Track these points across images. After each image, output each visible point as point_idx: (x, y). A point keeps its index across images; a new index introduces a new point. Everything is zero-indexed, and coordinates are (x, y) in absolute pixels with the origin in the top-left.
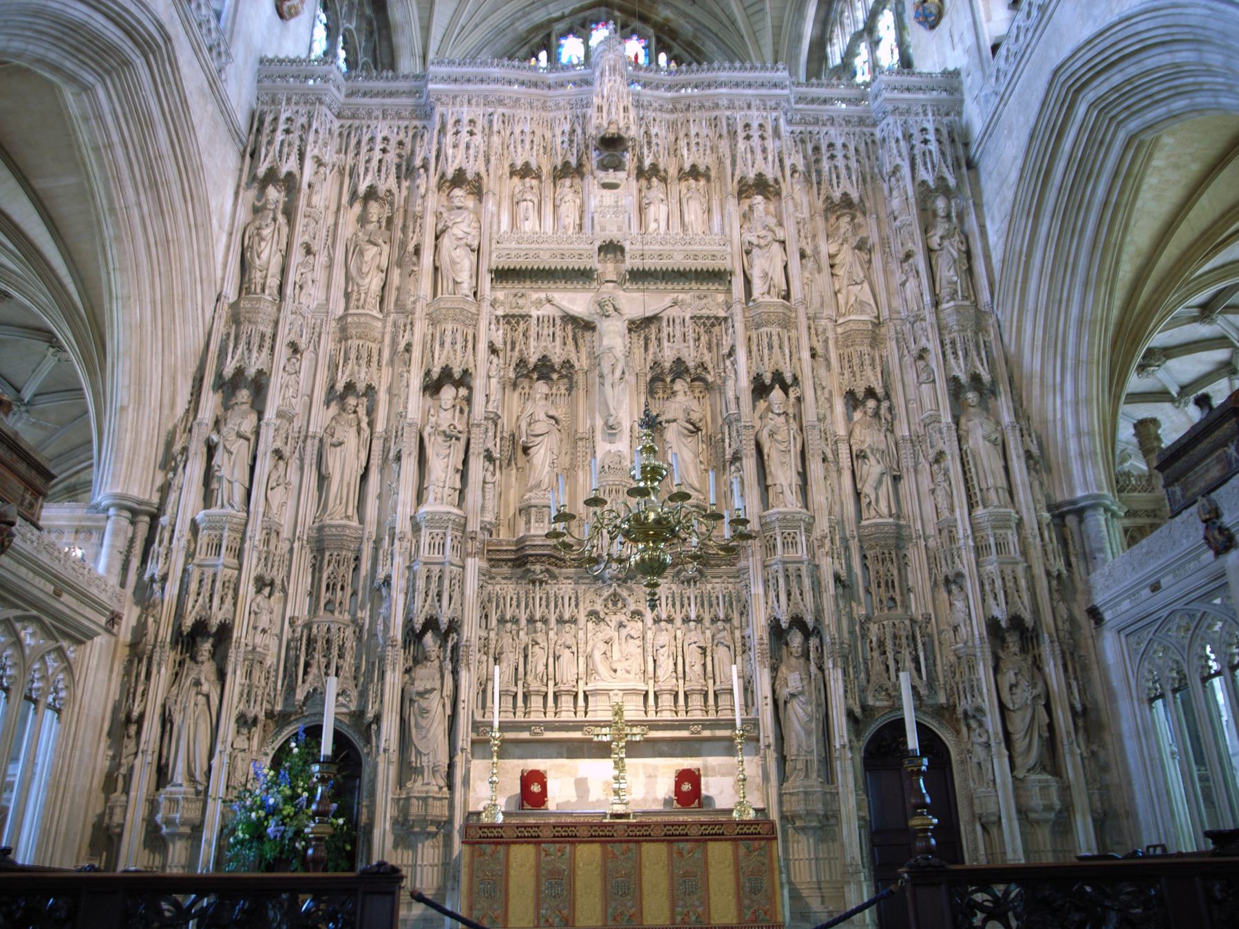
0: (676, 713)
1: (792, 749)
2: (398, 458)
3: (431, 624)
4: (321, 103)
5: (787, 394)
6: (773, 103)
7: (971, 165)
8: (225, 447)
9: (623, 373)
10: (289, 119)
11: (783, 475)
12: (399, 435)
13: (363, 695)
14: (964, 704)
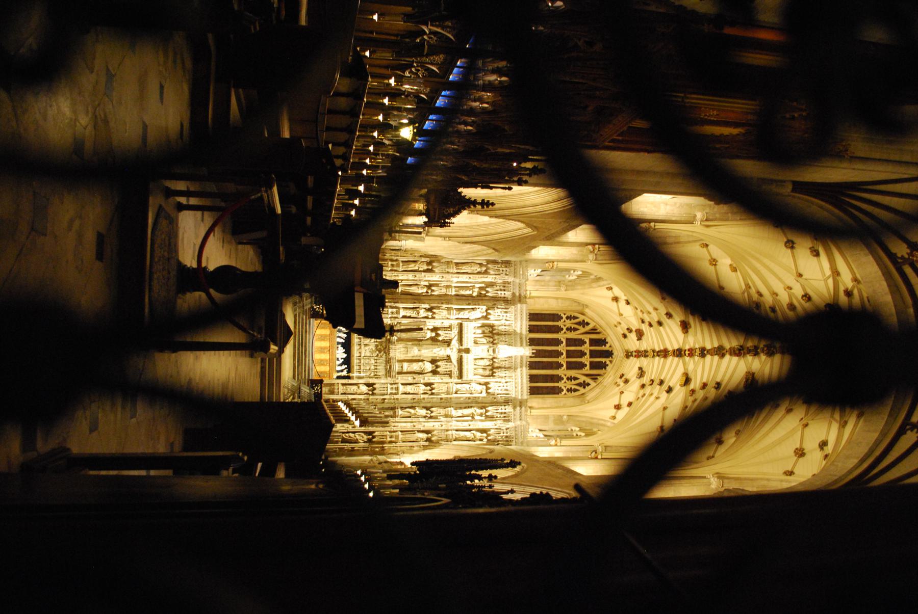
1: (348, 386)
2: (415, 303)
4: (515, 277)
11: (409, 389)
12: (419, 303)
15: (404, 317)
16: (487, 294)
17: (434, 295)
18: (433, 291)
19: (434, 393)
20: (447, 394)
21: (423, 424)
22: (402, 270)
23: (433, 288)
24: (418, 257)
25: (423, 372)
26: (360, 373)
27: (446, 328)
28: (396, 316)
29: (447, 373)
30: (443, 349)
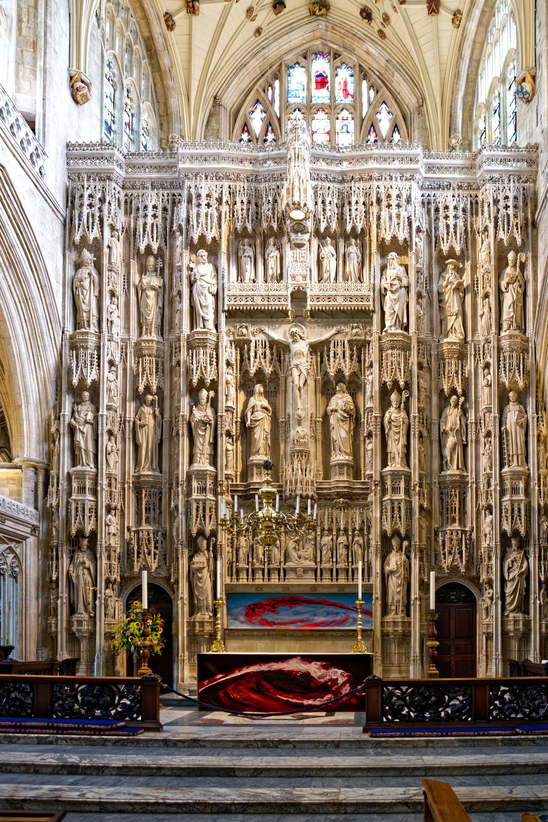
0: (332, 579)
2: (178, 434)
3: (201, 533)
4: (109, 179)
5: (401, 395)
6: (408, 176)
7: (535, 225)
8: (79, 429)
9: (306, 381)
10: (91, 196)
12: (177, 422)
13: (169, 570)
14: (484, 577)
15: (214, 461)
16: (155, 252)
17: (159, 388)
18: (148, 389)
19: (406, 383)
20: (410, 350)
21: (481, 414)
22: (92, 465)
23: (141, 388)
24: (59, 424)
25: (353, 413)
26: (357, 569)
27: (242, 355)
28: (209, 483)
29: (355, 352)
30: (295, 361)
